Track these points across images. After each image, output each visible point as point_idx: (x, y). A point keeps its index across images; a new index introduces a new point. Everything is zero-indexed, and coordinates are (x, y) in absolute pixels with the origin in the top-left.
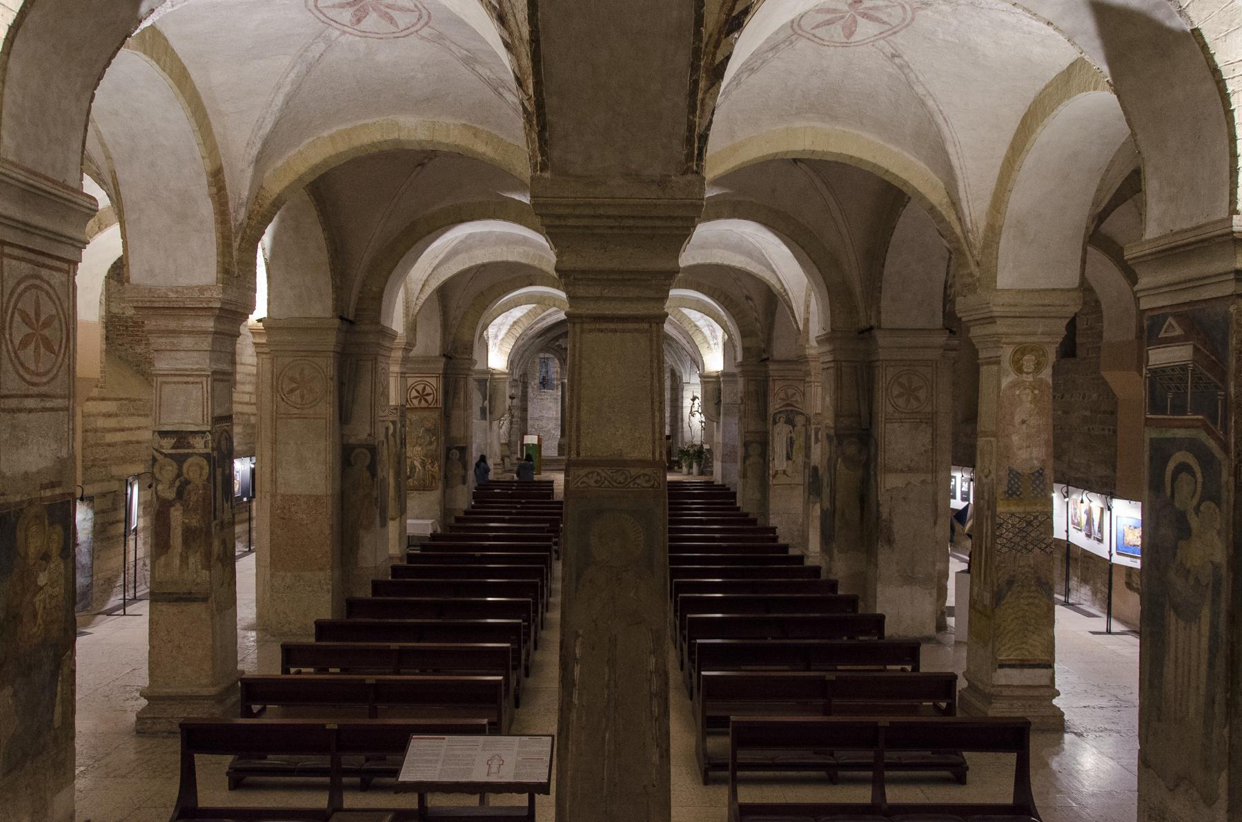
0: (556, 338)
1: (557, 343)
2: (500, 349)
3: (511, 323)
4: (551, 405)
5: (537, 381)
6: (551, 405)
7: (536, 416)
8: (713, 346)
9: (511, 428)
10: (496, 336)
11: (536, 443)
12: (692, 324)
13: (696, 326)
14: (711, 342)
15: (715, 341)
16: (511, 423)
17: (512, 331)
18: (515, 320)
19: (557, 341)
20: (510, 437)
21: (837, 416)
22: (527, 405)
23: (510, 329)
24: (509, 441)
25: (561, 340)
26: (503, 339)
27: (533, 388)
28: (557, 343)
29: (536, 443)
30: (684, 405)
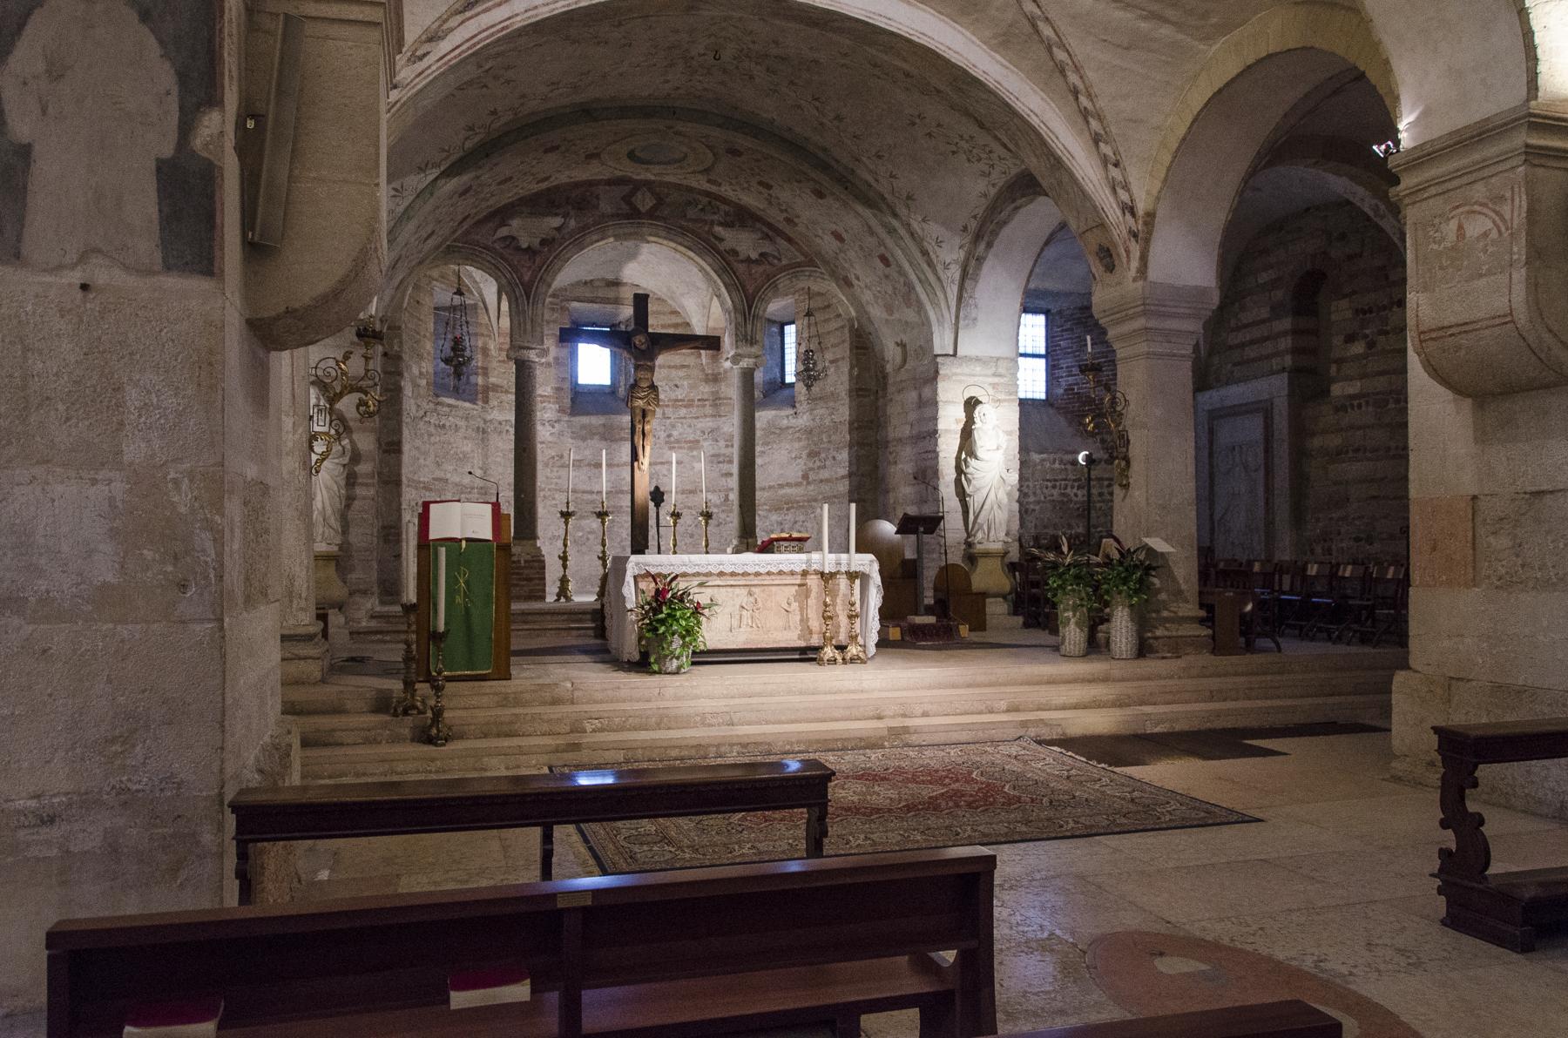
0: (502, 215)
1: (503, 232)
4: (467, 447)
5: (427, 366)
6: (467, 447)
7: (425, 477)
9: (350, 499)
11: (486, 533)
16: (351, 480)
19: (503, 224)
20: (345, 531)
21: (1024, 512)
22: (399, 432)
24: (345, 547)
25: (515, 223)
27: (416, 386)
28: (503, 232)
29: (486, 533)
30: (941, 426)
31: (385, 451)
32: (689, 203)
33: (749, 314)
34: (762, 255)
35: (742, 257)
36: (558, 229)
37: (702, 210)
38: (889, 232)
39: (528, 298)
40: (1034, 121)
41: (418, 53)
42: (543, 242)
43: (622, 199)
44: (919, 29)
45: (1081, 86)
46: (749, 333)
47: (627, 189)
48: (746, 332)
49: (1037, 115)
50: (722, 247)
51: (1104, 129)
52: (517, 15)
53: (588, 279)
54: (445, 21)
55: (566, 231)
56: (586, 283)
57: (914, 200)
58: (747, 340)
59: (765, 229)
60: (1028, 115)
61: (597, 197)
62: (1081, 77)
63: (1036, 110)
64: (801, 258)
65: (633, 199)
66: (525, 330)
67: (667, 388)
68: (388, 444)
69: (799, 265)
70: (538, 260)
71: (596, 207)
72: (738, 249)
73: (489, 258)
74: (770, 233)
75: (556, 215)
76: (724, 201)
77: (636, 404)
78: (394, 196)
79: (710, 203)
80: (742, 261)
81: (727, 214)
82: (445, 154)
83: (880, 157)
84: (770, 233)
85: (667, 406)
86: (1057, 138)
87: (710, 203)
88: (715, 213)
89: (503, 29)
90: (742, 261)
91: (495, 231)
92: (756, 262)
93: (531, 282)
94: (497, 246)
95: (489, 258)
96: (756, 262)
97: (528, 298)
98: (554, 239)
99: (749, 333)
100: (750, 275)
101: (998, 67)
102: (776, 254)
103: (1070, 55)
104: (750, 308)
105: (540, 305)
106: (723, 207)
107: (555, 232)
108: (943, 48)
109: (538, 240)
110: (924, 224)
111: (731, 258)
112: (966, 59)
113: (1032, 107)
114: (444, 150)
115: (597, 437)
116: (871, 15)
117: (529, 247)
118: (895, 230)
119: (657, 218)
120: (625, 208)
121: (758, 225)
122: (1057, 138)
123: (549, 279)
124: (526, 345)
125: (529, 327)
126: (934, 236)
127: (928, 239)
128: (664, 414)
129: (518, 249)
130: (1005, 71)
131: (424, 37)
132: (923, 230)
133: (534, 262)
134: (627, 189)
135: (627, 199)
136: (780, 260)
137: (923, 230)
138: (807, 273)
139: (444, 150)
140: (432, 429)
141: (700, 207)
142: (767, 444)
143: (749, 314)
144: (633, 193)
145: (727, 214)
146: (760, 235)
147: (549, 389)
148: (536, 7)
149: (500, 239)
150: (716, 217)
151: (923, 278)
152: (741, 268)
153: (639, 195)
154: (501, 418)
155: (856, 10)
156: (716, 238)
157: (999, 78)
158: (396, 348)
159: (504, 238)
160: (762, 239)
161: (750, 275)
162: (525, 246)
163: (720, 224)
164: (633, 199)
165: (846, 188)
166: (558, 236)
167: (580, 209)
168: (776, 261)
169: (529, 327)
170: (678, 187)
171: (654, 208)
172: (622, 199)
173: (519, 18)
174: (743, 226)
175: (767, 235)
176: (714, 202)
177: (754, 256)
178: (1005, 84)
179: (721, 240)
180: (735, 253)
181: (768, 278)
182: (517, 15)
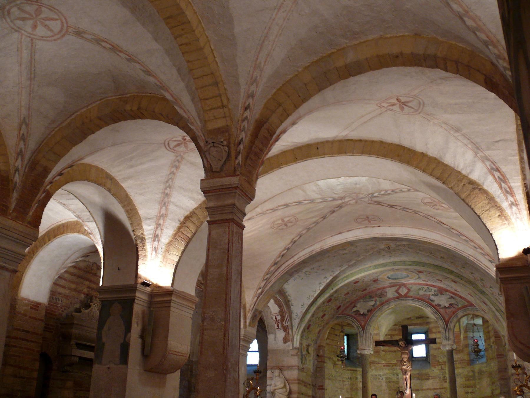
1: (355, 309)
2: (164, 257)
3: (182, 219)
8: (508, 211)
10: (156, 237)
12: (465, 181)
13: (472, 182)
14: (505, 205)
15: (510, 198)
17: (182, 230)
18: (188, 213)
19: (355, 306)
23: (179, 228)
25: (358, 305)
26: (170, 244)
28: (355, 309)
31: (318, 389)
32: (421, 289)
33: (447, 329)
34: (450, 304)
35: (442, 306)
36: (373, 306)
37: (425, 291)
38: (481, 293)
39: (364, 331)
40: (471, 258)
41: (265, 278)
42: (368, 311)
43: (395, 292)
44: (423, 236)
45: (476, 246)
46: (447, 336)
47: (396, 288)
48: (446, 335)
49: (472, 256)
50: (434, 304)
51: (492, 258)
52: (295, 260)
53: (409, 317)
54: (270, 269)
55: (376, 306)
56: (408, 319)
57: (484, 280)
58: (446, 339)
59: (451, 295)
60: (469, 257)
61: (386, 293)
62: (475, 243)
63: (472, 255)
64: (466, 304)
65: (399, 291)
66: (363, 343)
67: (442, 357)
68: (319, 386)
69: (466, 306)
70: (366, 317)
71: (386, 296)
72: (440, 303)
73: (350, 319)
74: (453, 296)
75: (372, 301)
76: (433, 286)
77: (403, 368)
78: (302, 307)
79: (428, 288)
80: (442, 308)
81: (435, 291)
82: (315, 292)
83: (464, 268)
84: (453, 296)
85: (443, 364)
86: (482, 263)
87: (428, 288)
88: (430, 291)
89: (292, 265)
90: (442, 308)
91: (352, 309)
92: (448, 308)
93: (365, 326)
94: (353, 314)
95: (350, 319)
96: (448, 308)
97: (364, 331)
98: (372, 309)
99: (447, 336)
100: (446, 313)
101: (455, 242)
102: (456, 303)
103: (467, 237)
104: (447, 326)
105: (368, 334)
106: (433, 289)
107: (372, 307)
108: (432, 240)
109: (367, 310)
110: (491, 289)
111: (438, 308)
112: (442, 242)
113: (470, 254)
114: (314, 291)
115: (416, 379)
116: (406, 236)
117: (364, 313)
118: (484, 292)
119: (409, 297)
120: (397, 295)
121: (447, 293)
122: (482, 263)
123: (370, 324)
124: (363, 348)
125: (364, 342)
126: (497, 293)
127: (495, 294)
128: (442, 368)
129: (360, 314)
130: (457, 243)
131: (265, 274)
132: (491, 291)
133: (365, 318)
134: (396, 288)
135: (397, 291)
136: (458, 305)
137: (491, 291)
138: (470, 309)
139: (314, 291)
140: (344, 379)
141: (424, 290)
142: (479, 379)
143: (447, 329)
144: (398, 289)
145: (435, 291)
146: (448, 297)
147: (395, 361)
148: (300, 257)
149: (353, 312)
150: (430, 293)
151: (498, 309)
152: (442, 311)
153: (401, 289)
154: (377, 373)
155: (400, 235)
156: (431, 300)
157: (455, 246)
158: (321, 353)
159: (355, 311)
160: (450, 298)
161: (446, 313)
162: (362, 313)
163: (433, 295)
164: (399, 291)
165: (461, 279)
166: (373, 308)
167: (380, 297)
168: (456, 306)
169: (364, 342)
170: (415, 284)
171: (407, 293)
172: (395, 292)
173: (296, 261)
174: (441, 294)
175: (452, 297)
176: (430, 287)
177: (447, 305)
178: (458, 247)
179: (434, 301)
180: (439, 305)
181: (454, 313)
182: (295, 260)
